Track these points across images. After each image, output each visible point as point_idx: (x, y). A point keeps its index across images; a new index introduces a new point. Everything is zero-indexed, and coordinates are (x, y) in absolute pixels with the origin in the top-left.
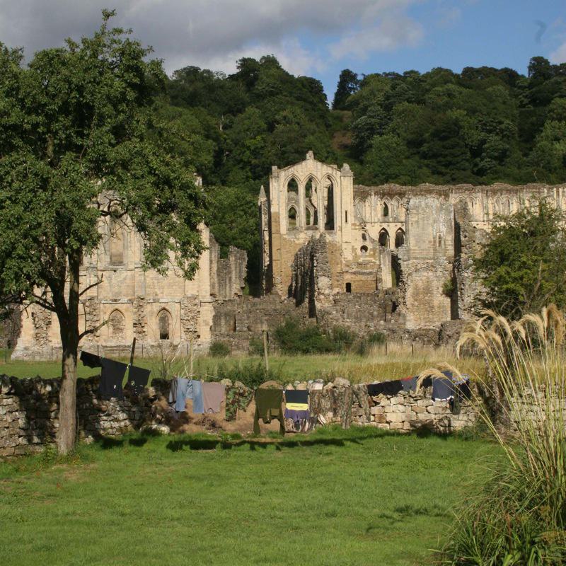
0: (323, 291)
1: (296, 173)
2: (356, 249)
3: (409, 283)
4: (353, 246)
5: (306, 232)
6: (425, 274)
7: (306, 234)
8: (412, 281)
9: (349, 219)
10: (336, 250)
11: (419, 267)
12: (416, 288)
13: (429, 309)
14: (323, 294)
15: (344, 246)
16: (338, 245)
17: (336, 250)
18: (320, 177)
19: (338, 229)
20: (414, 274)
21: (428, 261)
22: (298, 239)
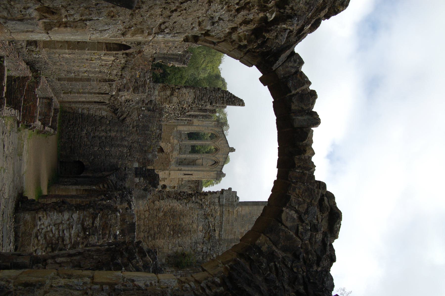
0: (176, 94)
1: (220, 139)
2: (164, 181)
3: (190, 205)
4: (166, 179)
5: (178, 144)
6: (200, 228)
7: (177, 144)
8: (191, 209)
9: (187, 176)
10: (164, 166)
11: (211, 219)
12: (182, 214)
13: (152, 232)
14: (172, 94)
15: (167, 172)
16: (168, 168)
17: (164, 166)
18: (217, 156)
19: (180, 168)
20: (201, 212)
21: (217, 232)
22: (173, 138)
